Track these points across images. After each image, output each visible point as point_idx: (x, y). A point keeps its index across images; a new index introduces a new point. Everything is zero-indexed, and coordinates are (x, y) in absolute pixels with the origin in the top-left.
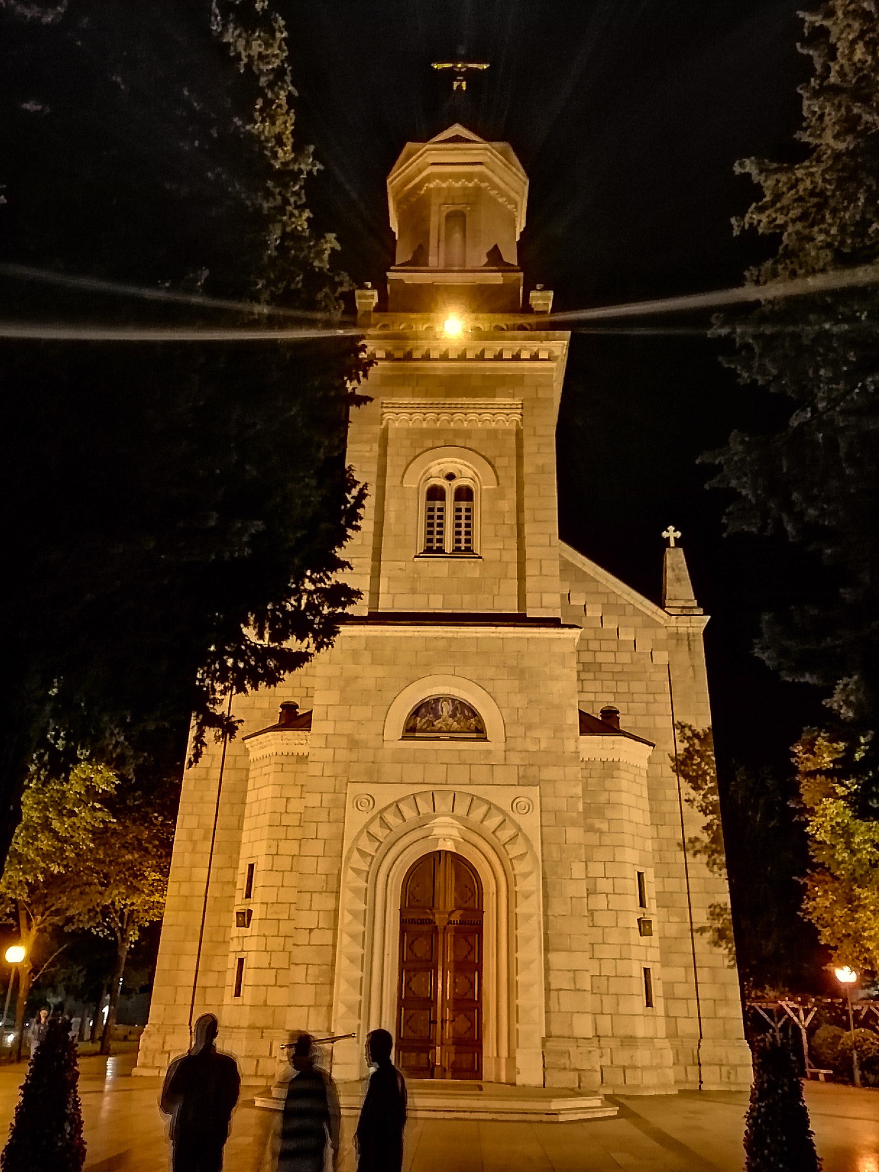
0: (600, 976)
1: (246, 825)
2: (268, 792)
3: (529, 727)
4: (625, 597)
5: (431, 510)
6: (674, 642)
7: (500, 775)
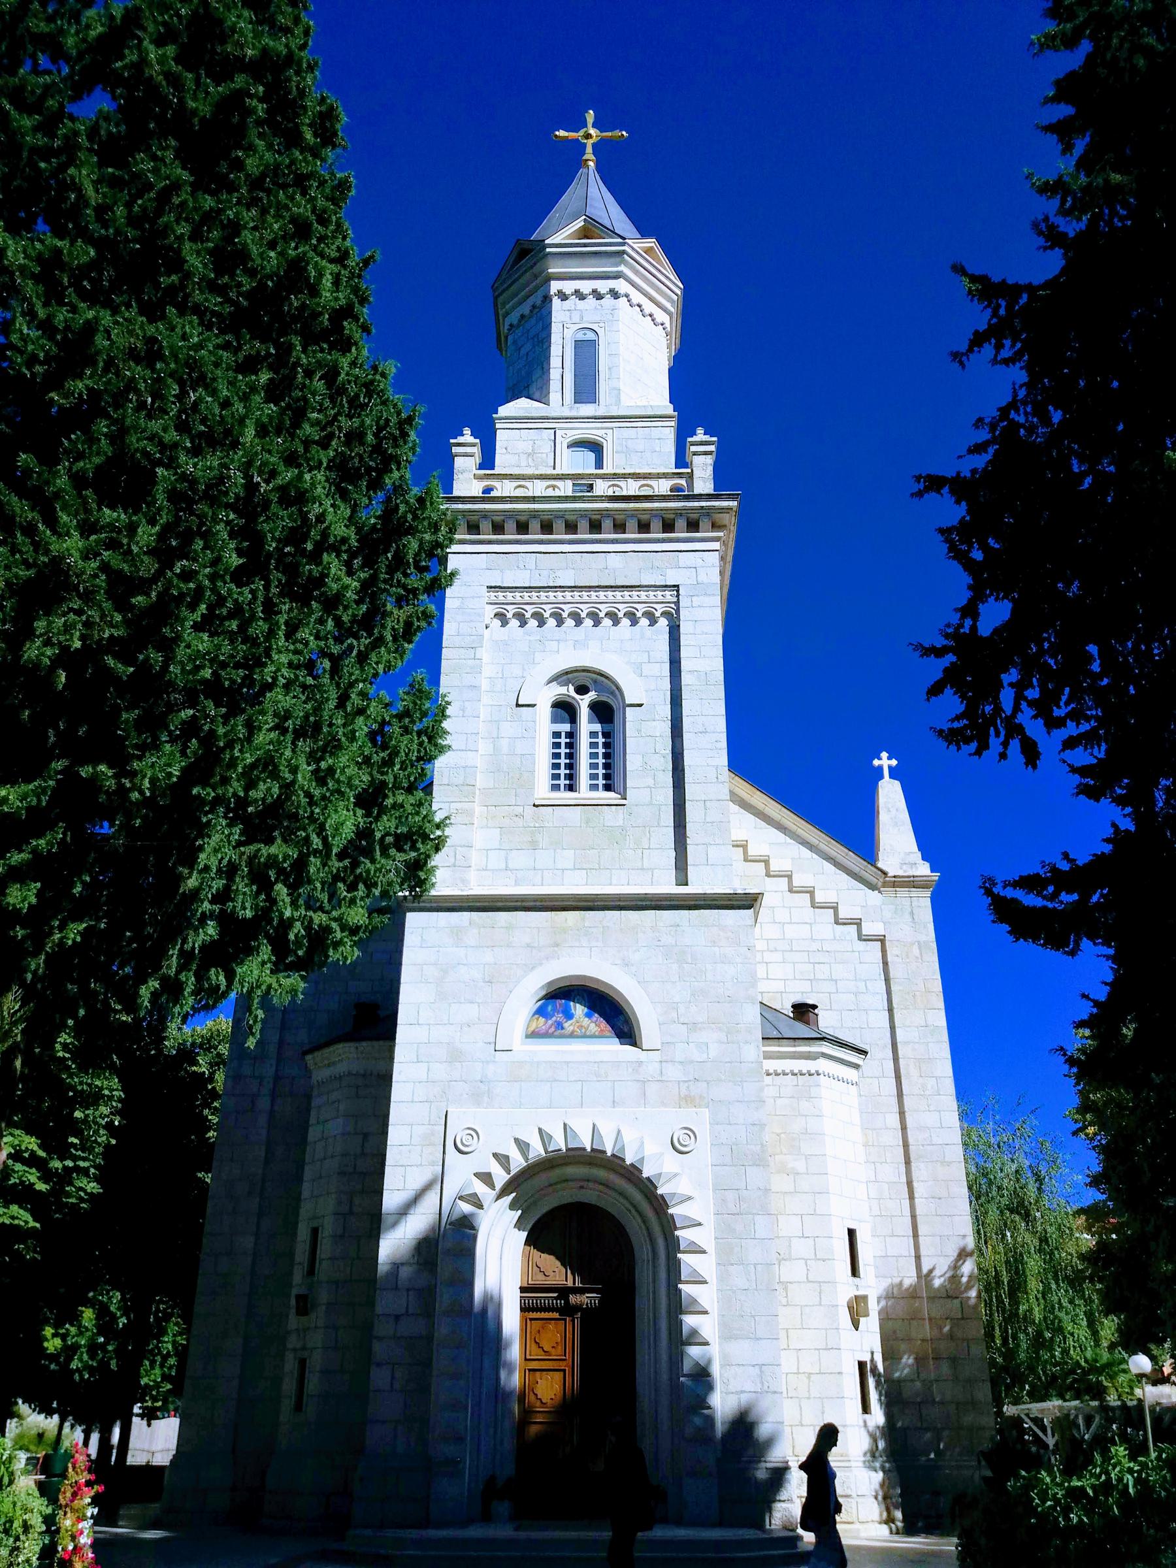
0: (798, 1373)
1: (308, 1173)
2: (335, 1127)
5: (557, 735)
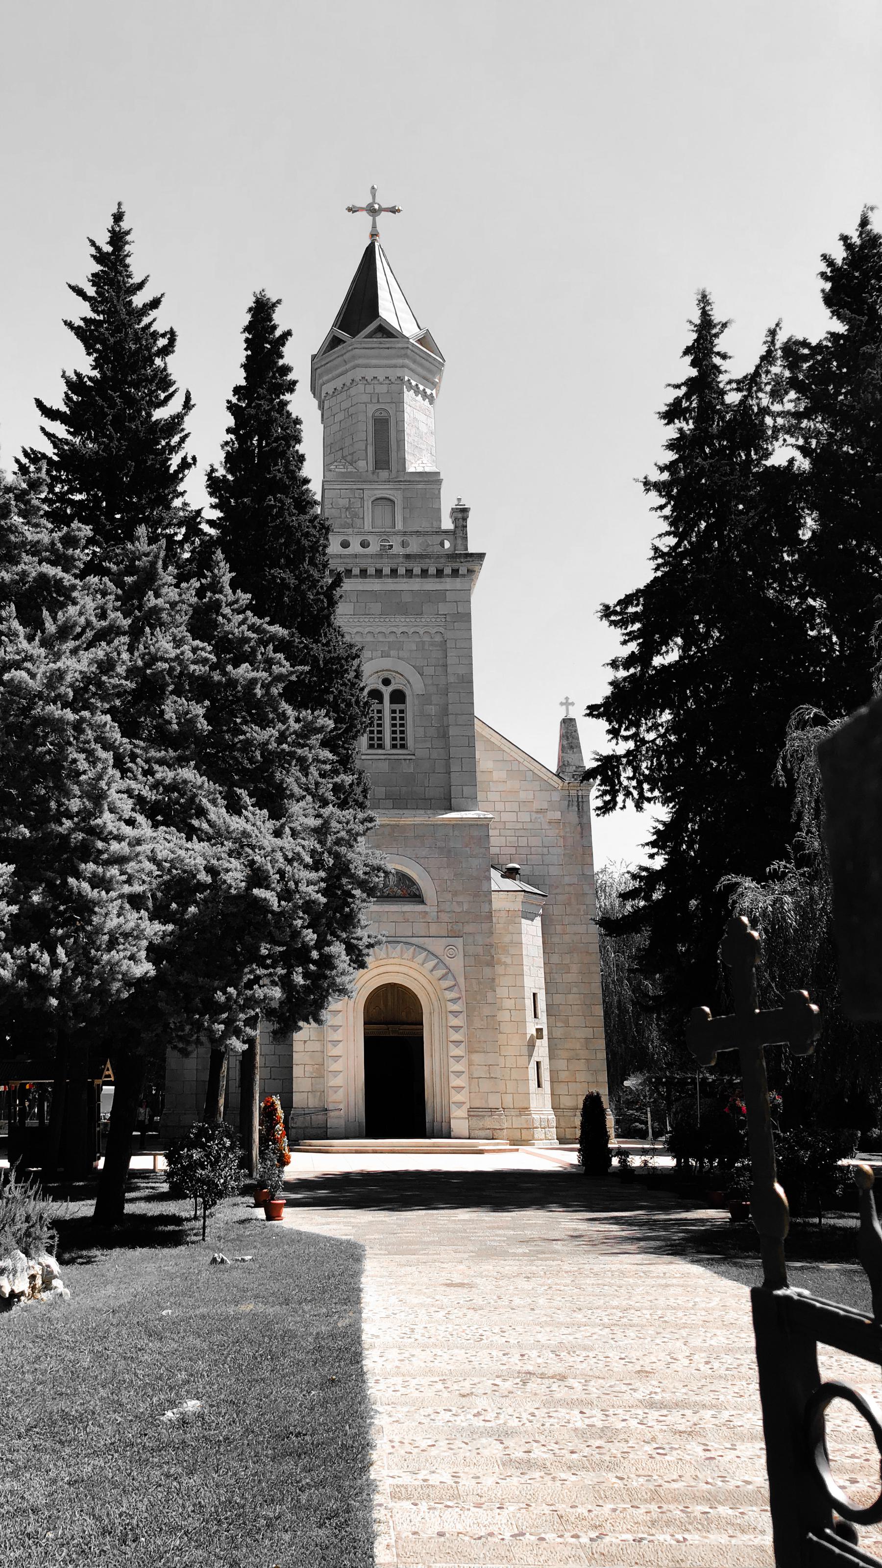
3: (455, 894)
4: (525, 763)
6: (567, 803)
7: (434, 929)
